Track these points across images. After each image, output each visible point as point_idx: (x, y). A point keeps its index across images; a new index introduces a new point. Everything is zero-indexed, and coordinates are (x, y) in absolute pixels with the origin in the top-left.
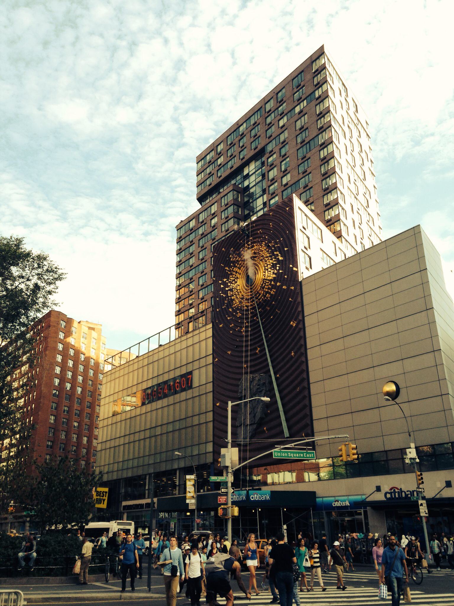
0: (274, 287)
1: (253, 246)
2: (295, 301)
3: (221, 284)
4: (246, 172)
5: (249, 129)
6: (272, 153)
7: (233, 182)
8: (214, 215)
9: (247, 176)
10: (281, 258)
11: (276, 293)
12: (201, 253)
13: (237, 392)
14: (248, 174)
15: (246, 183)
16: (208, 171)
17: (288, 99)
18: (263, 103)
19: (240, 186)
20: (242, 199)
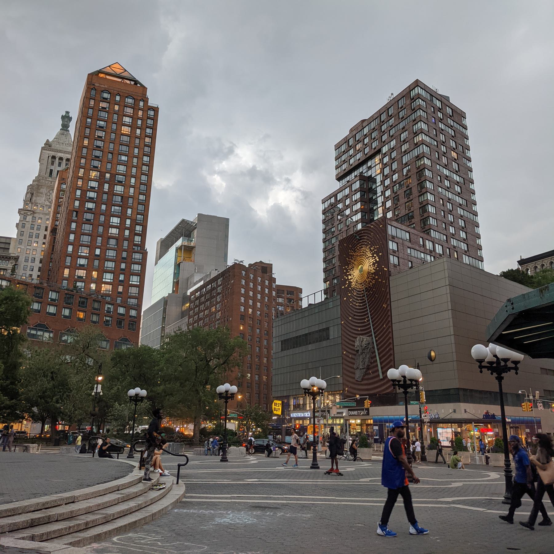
0: (374, 278)
1: (362, 247)
2: (386, 291)
3: (344, 269)
4: (369, 164)
5: (370, 132)
6: (385, 155)
7: (361, 170)
8: (347, 197)
9: (370, 168)
10: (378, 260)
11: (375, 282)
12: (339, 225)
13: (354, 346)
14: (371, 166)
15: (369, 173)
16: (343, 158)
17: (395, 115)
18: (379, 114)
19: (365, 175)
20: (367, 186)
